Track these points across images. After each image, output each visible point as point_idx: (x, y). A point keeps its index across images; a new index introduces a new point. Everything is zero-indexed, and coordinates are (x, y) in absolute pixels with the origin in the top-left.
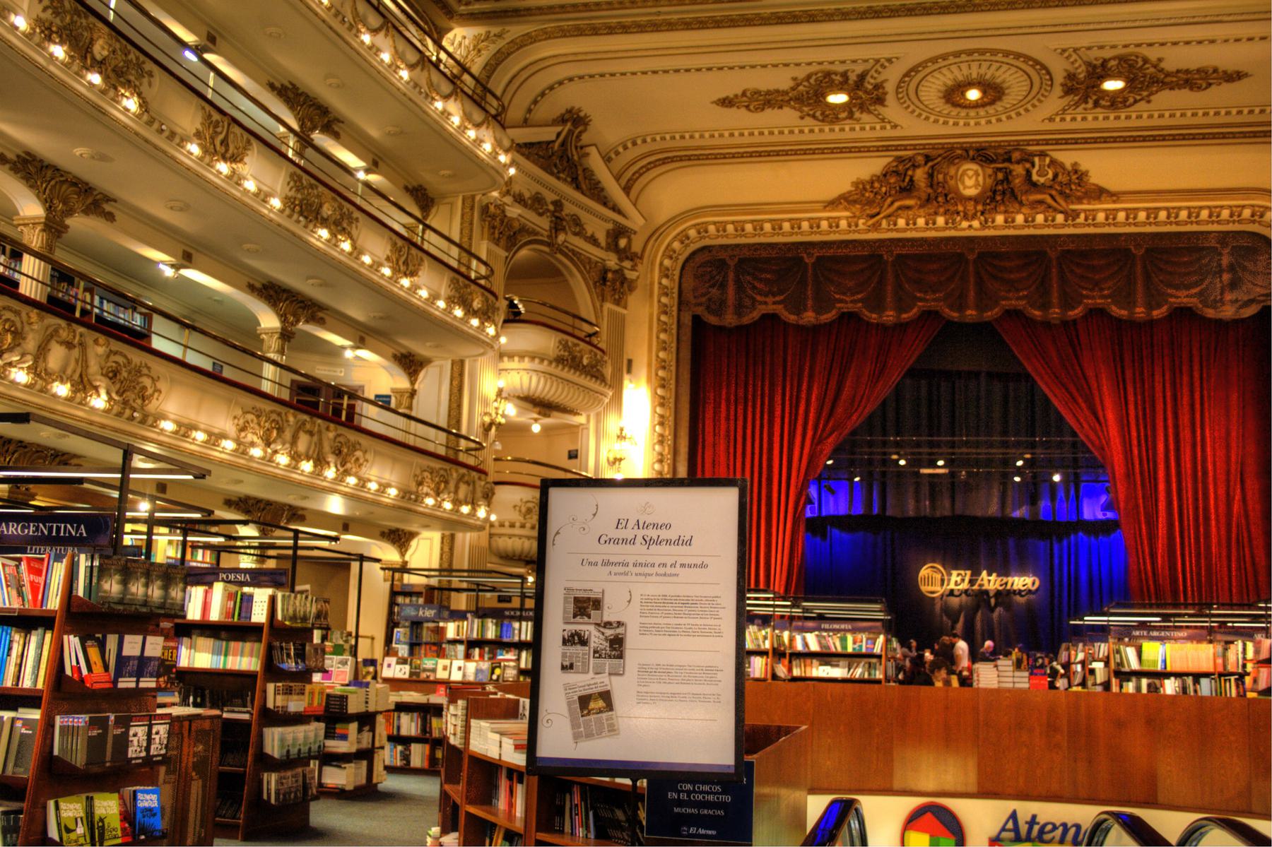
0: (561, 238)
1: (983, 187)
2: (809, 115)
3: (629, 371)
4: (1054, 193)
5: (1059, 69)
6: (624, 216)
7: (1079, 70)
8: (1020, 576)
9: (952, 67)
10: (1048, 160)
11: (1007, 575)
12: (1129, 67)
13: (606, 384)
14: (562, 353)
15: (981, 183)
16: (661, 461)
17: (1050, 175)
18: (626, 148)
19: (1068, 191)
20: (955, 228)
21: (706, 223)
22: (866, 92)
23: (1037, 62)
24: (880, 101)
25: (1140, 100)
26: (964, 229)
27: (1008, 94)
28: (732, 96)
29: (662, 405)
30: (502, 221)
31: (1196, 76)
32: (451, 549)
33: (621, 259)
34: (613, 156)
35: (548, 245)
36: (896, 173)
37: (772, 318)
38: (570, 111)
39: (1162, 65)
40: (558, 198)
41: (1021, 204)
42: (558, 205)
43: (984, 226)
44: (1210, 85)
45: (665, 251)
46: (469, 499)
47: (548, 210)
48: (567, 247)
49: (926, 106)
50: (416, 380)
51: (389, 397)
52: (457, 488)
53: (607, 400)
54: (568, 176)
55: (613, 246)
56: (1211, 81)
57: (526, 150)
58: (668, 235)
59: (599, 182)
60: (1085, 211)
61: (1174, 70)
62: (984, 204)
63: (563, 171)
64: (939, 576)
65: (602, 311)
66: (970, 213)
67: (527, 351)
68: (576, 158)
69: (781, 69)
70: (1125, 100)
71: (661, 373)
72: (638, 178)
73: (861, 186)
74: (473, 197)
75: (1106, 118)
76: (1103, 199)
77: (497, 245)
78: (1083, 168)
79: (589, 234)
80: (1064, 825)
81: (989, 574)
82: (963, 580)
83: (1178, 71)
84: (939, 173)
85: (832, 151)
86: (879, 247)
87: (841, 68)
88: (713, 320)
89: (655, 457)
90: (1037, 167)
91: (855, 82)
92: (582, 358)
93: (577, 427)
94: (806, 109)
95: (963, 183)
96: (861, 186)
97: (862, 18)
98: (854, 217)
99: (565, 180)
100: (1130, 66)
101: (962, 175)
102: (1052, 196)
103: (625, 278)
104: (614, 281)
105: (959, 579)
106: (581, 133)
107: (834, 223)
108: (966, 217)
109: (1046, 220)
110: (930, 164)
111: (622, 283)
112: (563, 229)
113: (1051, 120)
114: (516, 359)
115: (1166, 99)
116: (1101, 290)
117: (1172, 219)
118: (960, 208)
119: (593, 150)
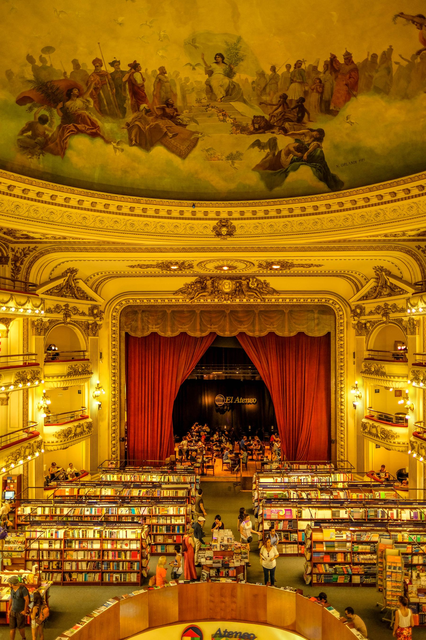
0: (68, 320)
4: (257, 292)
5: (256, 264)
10: (255, 279)
17: (256, 285)
23: (248, 262)
33: (95, 318)
36: (200, 282)
37: (154, 334)
41: (245, 295)
55: (92, 314)
77: (40, 335)
78: (267, 282)
86: (194, 307)
88: (133, 334)
96: (188, 286)
102: (256, 294)
104: (92, 328)
108: (225, 300)
111: (96, 327)
112: (70, 316)
116: (273, 325)
118: (223, 297)
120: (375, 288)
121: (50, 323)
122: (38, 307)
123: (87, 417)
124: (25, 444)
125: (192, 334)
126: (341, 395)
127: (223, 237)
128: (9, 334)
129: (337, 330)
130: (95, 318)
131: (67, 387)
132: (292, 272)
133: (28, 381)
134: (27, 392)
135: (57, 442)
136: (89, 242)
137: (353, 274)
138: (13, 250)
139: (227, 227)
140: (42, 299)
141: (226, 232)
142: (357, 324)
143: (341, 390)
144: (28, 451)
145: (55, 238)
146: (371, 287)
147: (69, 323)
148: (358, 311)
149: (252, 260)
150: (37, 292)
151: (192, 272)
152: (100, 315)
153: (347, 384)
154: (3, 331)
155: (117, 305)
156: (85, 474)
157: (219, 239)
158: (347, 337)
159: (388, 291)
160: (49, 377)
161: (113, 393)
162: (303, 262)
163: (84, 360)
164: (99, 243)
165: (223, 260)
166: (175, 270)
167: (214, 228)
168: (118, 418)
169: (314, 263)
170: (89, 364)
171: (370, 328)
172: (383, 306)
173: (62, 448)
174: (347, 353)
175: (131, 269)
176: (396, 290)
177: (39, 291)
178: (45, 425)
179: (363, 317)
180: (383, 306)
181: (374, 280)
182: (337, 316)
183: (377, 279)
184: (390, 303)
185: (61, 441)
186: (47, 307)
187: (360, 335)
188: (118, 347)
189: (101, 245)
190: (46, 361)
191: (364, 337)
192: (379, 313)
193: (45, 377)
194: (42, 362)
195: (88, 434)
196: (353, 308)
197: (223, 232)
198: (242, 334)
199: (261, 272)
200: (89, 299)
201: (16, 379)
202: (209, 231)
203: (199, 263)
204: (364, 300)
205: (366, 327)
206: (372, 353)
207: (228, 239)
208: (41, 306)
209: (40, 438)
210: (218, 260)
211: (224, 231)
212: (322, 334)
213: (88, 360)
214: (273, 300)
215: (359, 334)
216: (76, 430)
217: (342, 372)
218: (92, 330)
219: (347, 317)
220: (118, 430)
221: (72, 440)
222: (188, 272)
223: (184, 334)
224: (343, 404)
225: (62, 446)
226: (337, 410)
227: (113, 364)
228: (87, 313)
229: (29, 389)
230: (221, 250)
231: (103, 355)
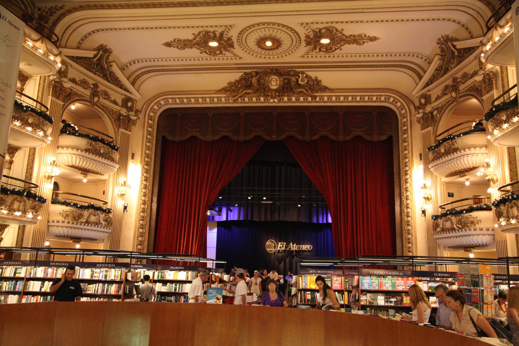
0: (96, 99)
1: (279, 86)
2: (204, 52)
3: (133, 158)
4: (307, 88)
5: (302, 32)
6: (130, 93)
7: (310, 34)
9: (258, 30)
10: (305, 75)
11: (300, 245)
12: (330, 32)
13: (114, 162)
14: (89, 147)
15: (278, 84)
16: (145, 196)
17: (306, 81)
19: (313, 88)
20: (268, 102)
24: (232, 46)
25: (338, 49)
26: (271, 103)
27: (283, 44)
28: (170, 42)
29: (146, 173)
30: (61, 90)
31: (358, 38)
32: (23, 232)
33: (128, 111)
35: (90, 102)
36: (245, 79)
38: (102, 46)
39: (344, 32)
42: (96, 86)
43: (279, 101)
44: (364, 42)
47: (90, 87)
48: (100, 104)
49: (251, 49)
50: (14, 156)
52: (12, 203)
53: (116, 170)
54: (101, 73)
56: (364, 41)
59: (118, 78)
60: (319, 96)
61: (349, 35)
62: (279, 93)
63: (98, 71)
64: (273, 245)
65: (118, 132)
66: (274, 96)
67: (71, 146)
68: (106, 66)
69: (186, 30)
70: (331, 49)
71: (146, 159)
72: (138, 78)
73: (231, 85)
75: (325, 57)
76: (326, 91)
78: (319, 79)
79: (113, 99)
81: (293, 244)
82: (283, 246)
83: (351, 36)
84: (262, 80)
85: (217, 69)
87: (212, 30)
88: (170, 138)
89: (142, 194)
90: (301, 78)
91: (219, 36)
92: (100, 150)
93: (105, 181)
94: (202, 49)
97: (215, 5)
98: (228, 97)
99: (99, 75)
100: (330, 32)
101: (271, 80)
102: (306, 90)
103: (131, 119)
105: (281, 246)
107: (220, 99)
108: (272, 98)
109: (304, 100)
110: (258, 76)
111: (129, 121)
113: (303, 57)
114: (65, 148)
115: (348, 48)
117: (354, 100)
118: (270, 94)
119: (114, 64)
135: (63, 222)
142: (422, 117)
146: (435, 67)
148: (423, 101)
160: (63, 147)
161: (143, 198)
171: (438, 115)
172: (451, 83)
178: (52, 203)
179: (428, 106)
180: (451, 83)
181: (439, 57)
183: (442, 56)
184: (459, 75)
187: (427, 127)
191: (430, 128)
192: (446, 94)
195: (105, 230)
198: (291, 137)
203: (240, 34)
205: (432, 116)
212: (384, 138)
214: (326, 99)
216: (89, 217)
221: (82, 227)
226: (403, 223)
228: (120, 102)
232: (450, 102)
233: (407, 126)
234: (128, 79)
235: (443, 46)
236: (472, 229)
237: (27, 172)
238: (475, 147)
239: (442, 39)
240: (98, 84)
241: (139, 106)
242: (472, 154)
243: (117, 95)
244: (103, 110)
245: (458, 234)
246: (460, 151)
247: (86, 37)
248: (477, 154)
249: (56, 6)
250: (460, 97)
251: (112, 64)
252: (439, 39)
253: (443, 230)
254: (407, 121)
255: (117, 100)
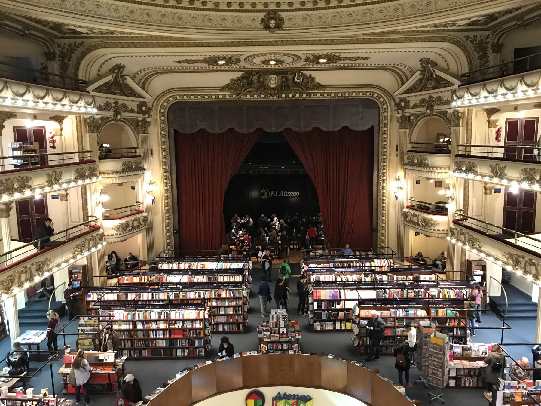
0: (119, 117)
4: (302, 87)
5: (303, 57)
6: (144, 98)
8: (293, 192)
10: (301, 74)
17: (301, 80)
18: (141, 72)
19: (307, 85)
21: (176, 95)
22: (233, 61)
23: (295, 55)
24: (239, 62)
33: (144, 115)
34: (136, 75)
37: (202, 131)
38: (116, 65)
40: (115, 100)
41: (291, 90)
42: (116, 103)
45: (161, 106)
46: (94, 244)
47: (112, 107)
51: (57, 196)
52: (89, 244)
55: (140, 111)
57: (98, 90)
58: (161, 101)
62: (278, 91)
68: (121, 82)
74: (80, 116)
77: (93, 132)
78: (313, 76)
80: (294, 395)
81: (283, 192)
82: (275, 194)
95: (270, 82)
96: (233, 81)
99: (118, 93)
104: (142, 125)
106: (122, 71)
108: (271, 95)
109: (300, 96)
110: (258, 74)
111: (145, 124)
112: (120, 113)
114: (106, 174)
119: (128, 78)
120: (420, 81)
121: (101, 120)
122: (91, 104)
123: (143, 212)
124: (89, 237)
125: (239, 131)
126: (383, 186)
127: (271, 30)
128: (63, 132)
129: (381, 124)
130: (144, 115)
131: (122, 183)
132: (338, 65)
133: (87, 177)
134: (85, 187)
135: (116, 235)
136: (137, 37)
137: (399, 67)
138: (59, 46)
139: (275, 20)
140: (93, 97)
141: (274, 25)
143: (383, 182)
144: (91, 243)
145: (102, 33)
146: (416, 80)
147: (120, 121)
148: (403, 104)
149: (299, 54)
150: (88, 89)
151: (238, 67)
152: (148, 111)
153: (389, 177)
154: (57, 129)
155: (164, 102)
156: (144, 264)
157: (267, 32)
158: (390, 130)
159: (434, 84)
160: (104, 174)
161: (165, 188)
162: (351, 55)
163: (136, 156)
164: (148, 37)
165: (270, 54)
166: (222, 65)
167: (262, 20)
168: (171, 212)
169: (361, 55)
170: (142, 160)
171: (414, 121)
172: (427, 98)
173: (121, 240)
174: (390, 146)
175: (179, 65)
176: (442, 82)
177: (90, 88)
178: (104, 220)
179: (407, 111)
180: (427, 98)
181: (420, 72)
182: (381, 109)
184: (435, 96)
185: (120, 234)
186: (98, 104)
187: (404, 128)
188: (168, 143)
189: (148, 40)
190: (100, 158)
191: (408, 130)
192: (423, 106)
193: (100, 173)
194: (97, 159)
196: (397, 101)
197: (271, 25)
198: (288, 129)
199: (307, 66)
200: (137, 95)
201: (75, 176)
202: (258, 24)
204: (408, 93)
205: (410, 119)
206: (415, 145)
207: (277, 32)
208: (93, 103)
209: (101, 231)
210: (266, 54)
211: (272, 23)
213: (140, 156)
214: (319, 95)
215: (402, 127)
216: (133, 224)
217: (385, 164)
218: (142, 127)
219: (391, 111)
220: (172, 223)
221: (130, 233)
222: (234, 67)
223: (231, 130)
224: (385, 195)
225: (122, 239)
226: (379, 200)
227: (164, 161)
228: (136, 110)
229: (87, 186)
230: (269, 44)
231: (154, 151)
232: (426, 114)
233: (388, 120)
234: (138, 84)
235: (424, 64)
236: (433, 229)
237: (83, 203)
238: (441, 168)
239: (423, 60)
240: (118, 101)
241: (150, 105)
242: (439, 172)
243: (132, 103)
244: (125, 122)
245: (421, 228)
246: (429, 169)
247: (104, 63)
248: (442, 173)
249: (75, 43)
250: (434, 115)
251: (126, 77)
252: (422, 59)
253: (411, 221)
254: (388, 115)
255: (133, 108)
